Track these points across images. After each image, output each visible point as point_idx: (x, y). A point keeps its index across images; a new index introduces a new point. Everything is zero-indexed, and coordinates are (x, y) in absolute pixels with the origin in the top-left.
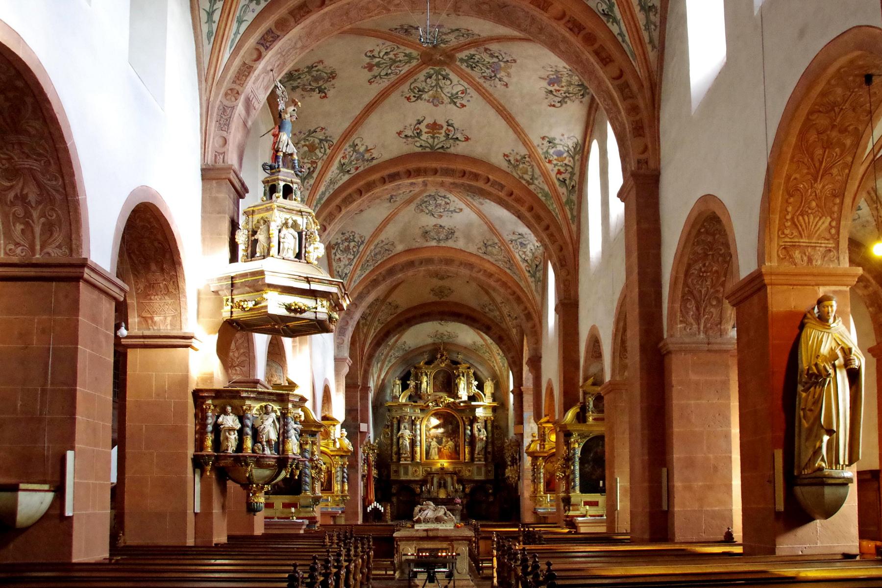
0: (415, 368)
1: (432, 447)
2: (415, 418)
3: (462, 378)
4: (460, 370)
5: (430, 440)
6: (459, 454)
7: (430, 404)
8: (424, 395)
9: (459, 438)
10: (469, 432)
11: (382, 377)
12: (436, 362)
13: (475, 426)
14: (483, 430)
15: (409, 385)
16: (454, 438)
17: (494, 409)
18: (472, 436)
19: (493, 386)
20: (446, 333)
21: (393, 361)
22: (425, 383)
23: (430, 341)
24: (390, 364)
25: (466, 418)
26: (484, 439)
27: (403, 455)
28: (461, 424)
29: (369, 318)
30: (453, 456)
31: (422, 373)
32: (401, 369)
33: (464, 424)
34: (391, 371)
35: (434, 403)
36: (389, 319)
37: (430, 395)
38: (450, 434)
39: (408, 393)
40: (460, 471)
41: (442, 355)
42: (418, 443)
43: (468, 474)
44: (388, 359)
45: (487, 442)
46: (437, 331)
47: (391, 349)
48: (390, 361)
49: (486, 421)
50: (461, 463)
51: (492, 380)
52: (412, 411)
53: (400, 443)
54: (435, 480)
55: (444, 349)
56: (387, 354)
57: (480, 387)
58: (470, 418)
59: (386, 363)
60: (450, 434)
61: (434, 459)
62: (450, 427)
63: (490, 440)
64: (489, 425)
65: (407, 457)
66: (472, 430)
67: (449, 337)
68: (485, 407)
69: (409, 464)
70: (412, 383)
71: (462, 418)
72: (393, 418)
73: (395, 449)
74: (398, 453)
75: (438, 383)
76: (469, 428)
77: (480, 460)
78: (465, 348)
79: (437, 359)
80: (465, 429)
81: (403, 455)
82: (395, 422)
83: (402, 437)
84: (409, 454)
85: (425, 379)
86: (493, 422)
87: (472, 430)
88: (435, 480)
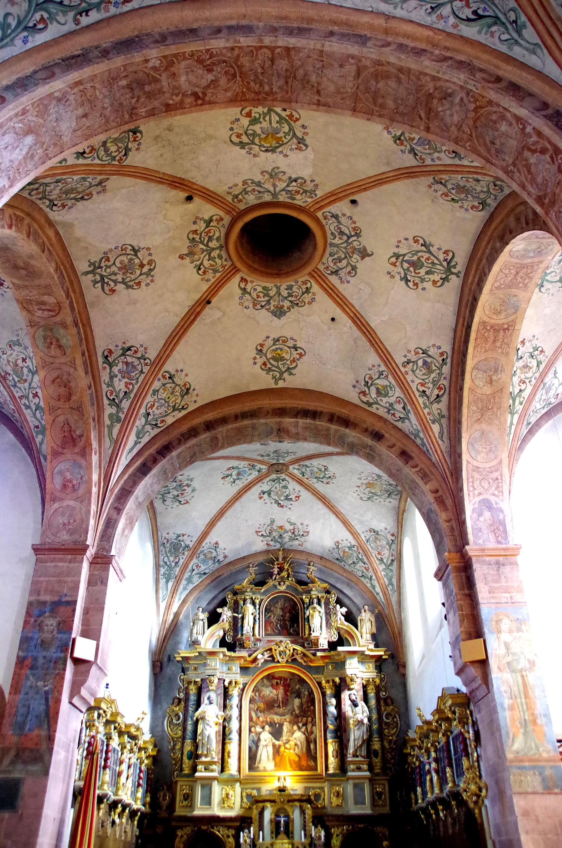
0: (235, 593)
1: (262, 743)
2: (230, 683)
3: (318, 607)
4: (314, 593)
5: (259, 729)
6: (315, 759)
7: (260, 656)
8: (248, 639)
9: (314, 724)
10: (332, 710)
11: (175, 608)
12: (271, 583)
13: (345, 695)
14: (361, 704)
15: (220, 615)
16: (305, 724)
17: (379, 662)
18: (341, 717)
19: (373, 620)
20: (288, 527)
21: (196, 580)
22: (252, 618)
23: (260, 545)
24: (191, 587)
25: (328, 682)
26: (366, 721)
27: (203, 759)
28: (317, 696)
29: (126, 404)
30: (304, 763)
31: (245, 600)
32: (211, 596)
33: (324, 694)
34: (191, 598)
35: (267, 655)
36: (170, 420)
37: (259, 640)
38: (297, 716)
39: (217, 631)
40: (317, 796)
41: (281, 569)
42: (234, 736)
43: (335, 801)
44: (187, 575)
45: (370, 727)
46: (273, 522)
47: (191, 558)
48: (189, 580)
49: (365, 687)
50: (318, 778)
51: (372, 612)
52: (225, 668)
53: (199, 731)
54: (268, 815)
55: (284, 558)
56: (186, 566)
57: (350, 618)
58: (333, 681)
59: (184, 582)
60: (297, 716)
61: (265, 770)
62: (297, 701)
63: (375, 727)
64: (372, 695)
65: (212, 763)
66: (339, 706)
67: (295, 536)
68: (363, 658)
69: (215, 778)
70: (226, 613)
71: (320, 684)
72: (189, 683)
73: (188, 747)
74: (194, 756)
75: (273, 619)
76: (334, 701)
77: (359, 769)
78: (321, 558)
79: (271, 575)
80: (325, 705)
81: (203, 759)
82: (193, 690)
83: (203, 718)
84: (216, 757)
85: (250, 608)
86: (378, 689)
87: (339, 706)
88: (268, 815)
